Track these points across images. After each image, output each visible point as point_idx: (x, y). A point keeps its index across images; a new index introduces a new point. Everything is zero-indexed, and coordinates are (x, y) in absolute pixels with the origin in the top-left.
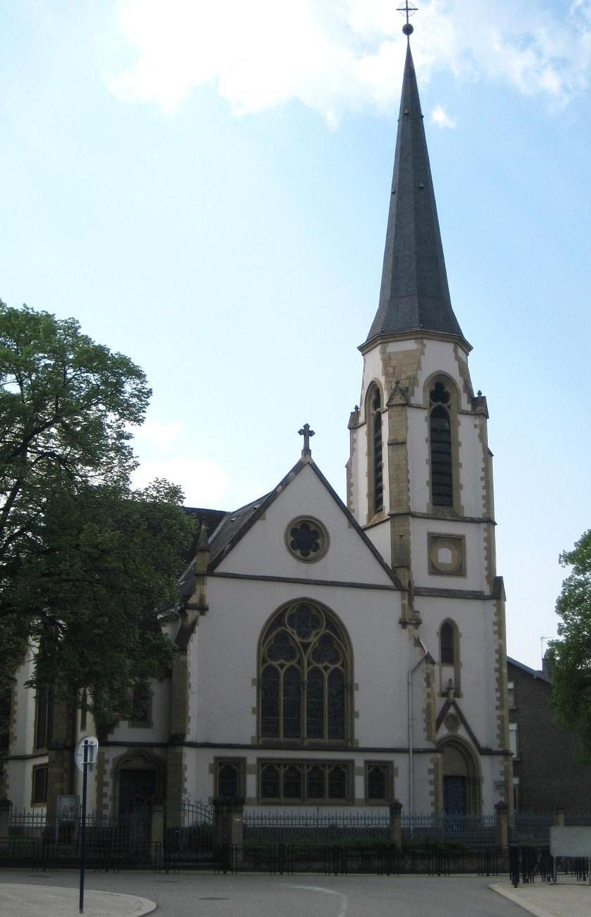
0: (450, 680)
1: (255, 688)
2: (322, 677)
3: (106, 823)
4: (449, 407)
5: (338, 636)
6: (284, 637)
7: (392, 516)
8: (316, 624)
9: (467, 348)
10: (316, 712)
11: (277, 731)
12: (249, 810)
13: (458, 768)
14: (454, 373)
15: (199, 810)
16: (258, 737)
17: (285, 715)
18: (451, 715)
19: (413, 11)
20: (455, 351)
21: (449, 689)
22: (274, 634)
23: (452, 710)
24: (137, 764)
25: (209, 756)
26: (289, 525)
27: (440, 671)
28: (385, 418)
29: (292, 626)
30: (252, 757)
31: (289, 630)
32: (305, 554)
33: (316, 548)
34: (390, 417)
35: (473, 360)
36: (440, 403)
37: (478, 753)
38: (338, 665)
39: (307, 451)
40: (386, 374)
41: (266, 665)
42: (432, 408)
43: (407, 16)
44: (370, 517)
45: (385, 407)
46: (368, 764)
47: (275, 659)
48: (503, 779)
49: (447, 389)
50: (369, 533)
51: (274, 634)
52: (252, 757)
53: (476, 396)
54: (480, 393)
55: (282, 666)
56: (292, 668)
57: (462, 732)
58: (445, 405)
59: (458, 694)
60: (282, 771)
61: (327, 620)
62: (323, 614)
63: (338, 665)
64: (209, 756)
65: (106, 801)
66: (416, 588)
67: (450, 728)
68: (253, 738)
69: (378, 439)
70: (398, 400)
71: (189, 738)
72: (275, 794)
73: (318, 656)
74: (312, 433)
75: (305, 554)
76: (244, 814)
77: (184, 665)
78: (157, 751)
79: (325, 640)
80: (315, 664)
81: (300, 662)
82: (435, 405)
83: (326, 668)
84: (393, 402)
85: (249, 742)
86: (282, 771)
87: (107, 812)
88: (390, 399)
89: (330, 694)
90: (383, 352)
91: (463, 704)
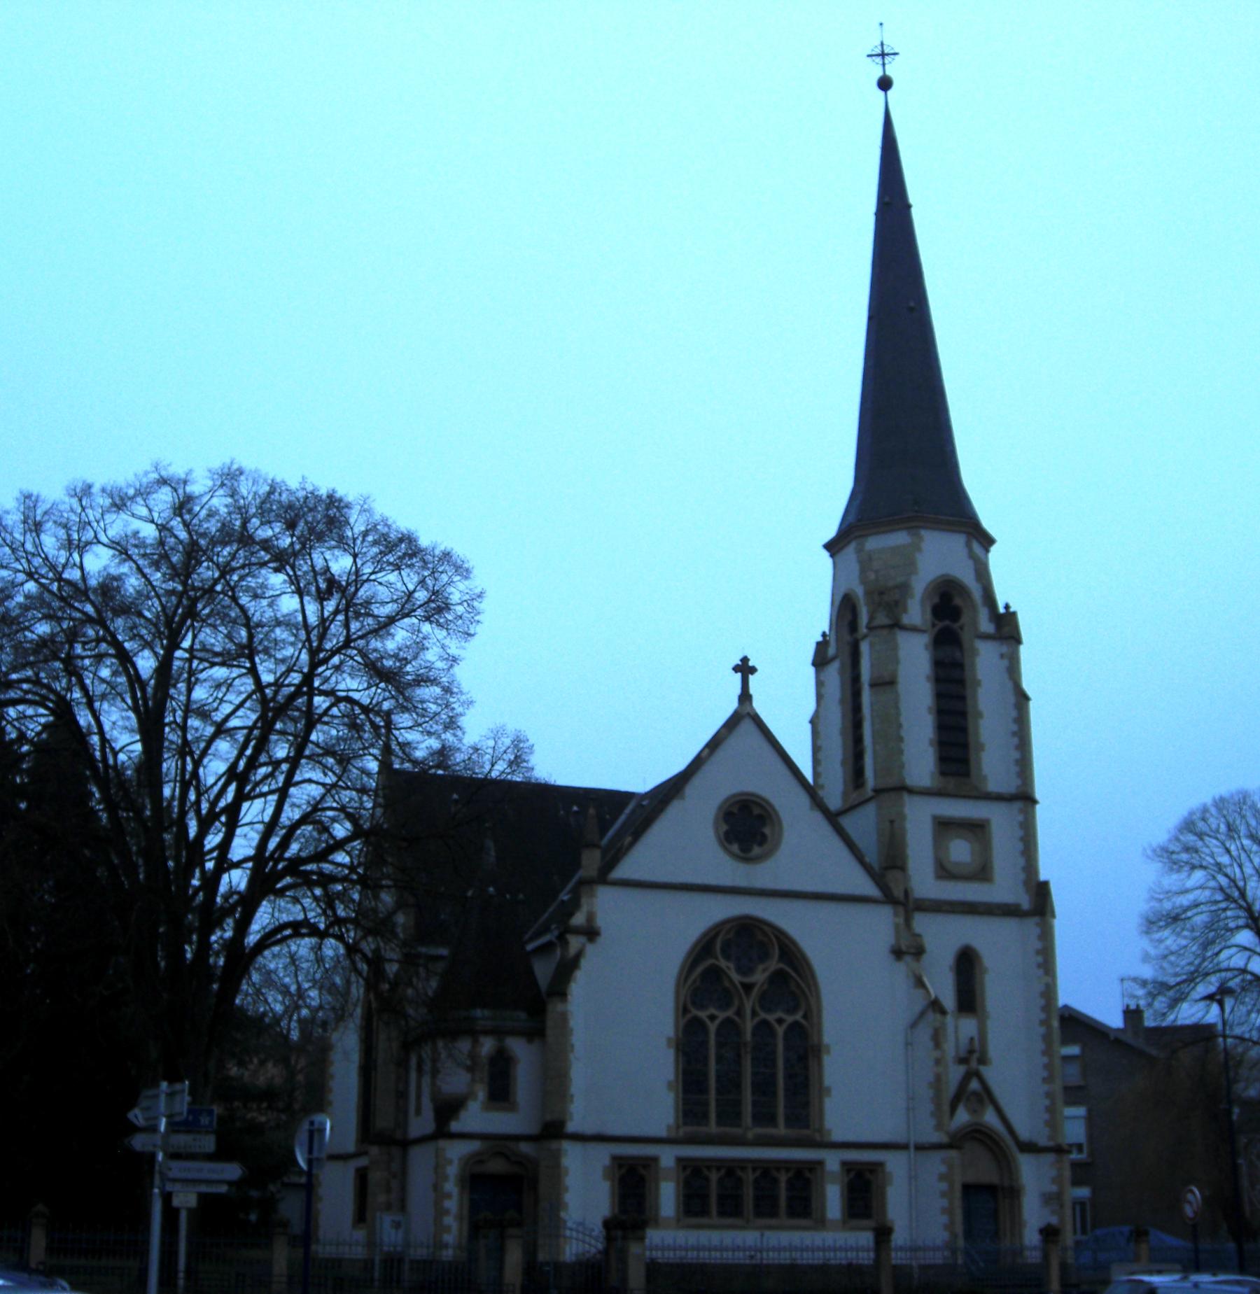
0: (972, 1039)
1: (672, 1052)
2: (773, 1034)
3: (448, 1254)
4: (961, 628)
5: (799, 975)
6: (714, 974)
7: (878, 791)
8: (764, 956)
9: (987, 541)
10: (764, 1087)
11: (705, 1116)
12: (654, 1236)
13: (985, 1172)
14: (967, 576)
15: (581, 1236)
16: (678, 1127)
17: (719, 1092)
18: (975, 1093)
19: (892, 56)
20: (968, 545)
21: (971, 1052)
22: (700, 969)
23: (974, 1085)
24: (497, 1166)
25: (602, 1155)
26: (720, 808)
27: (956, 1028)
28: (864, 647)
29: (727, 957)
30: (667, 1157)
31: (723, 963)
32: (746, 849)
33: (763, 840)
34: (872, 646)
35: (995, 558)
36: (947, 623)
37: (1014, 1149)
38: (798, 1017)
39: (745, 697)
40: (863, 581)
41: (689, 1016)
42: (936, 629)
43: (884, 65)
44: (845, 794)
45: (865, 631)
46: (847, 1166)
47: (702, 1007)
48: (1054, 1188)
49: (958, 601)
50: (847, 822)
51: (700, 969)
52: (667, 1157)
53: (1002, 610)
54: (1007, 607)
55: (712, 1018)
56: (728, 1021)
57: (990, 1117)
58: (956, 626)
59: (983, 1060)
60: (714, 1176)
61: (781, 949)
62: (774, 940)
63: (798, 1017)
64: (602, 1155)
65: (449, 1220)
66: (917, 900)
67: (974, 1112)
68: (669, 1127)
69: (856, 679)
70: (882, 619)
71: (571, 1127)
72: (704, 1212)
73: (766, 1001)
74: (753, 670)
75: (746, 849)
76: (647, 1241)
77: (564, 1017)
78: (525, 1147)
79: (779, 978)
80: (763, 1015)
81: (739, 1013)
82: (940, 625)
83: (780, 1021)
84: (877, 622)
85: (662, 1132)
86: (714, 1176)
87: (449, 1238)
88: (871, 618)
89: (787, 1060)
90: (859, 551)
91: (988, 1073)
